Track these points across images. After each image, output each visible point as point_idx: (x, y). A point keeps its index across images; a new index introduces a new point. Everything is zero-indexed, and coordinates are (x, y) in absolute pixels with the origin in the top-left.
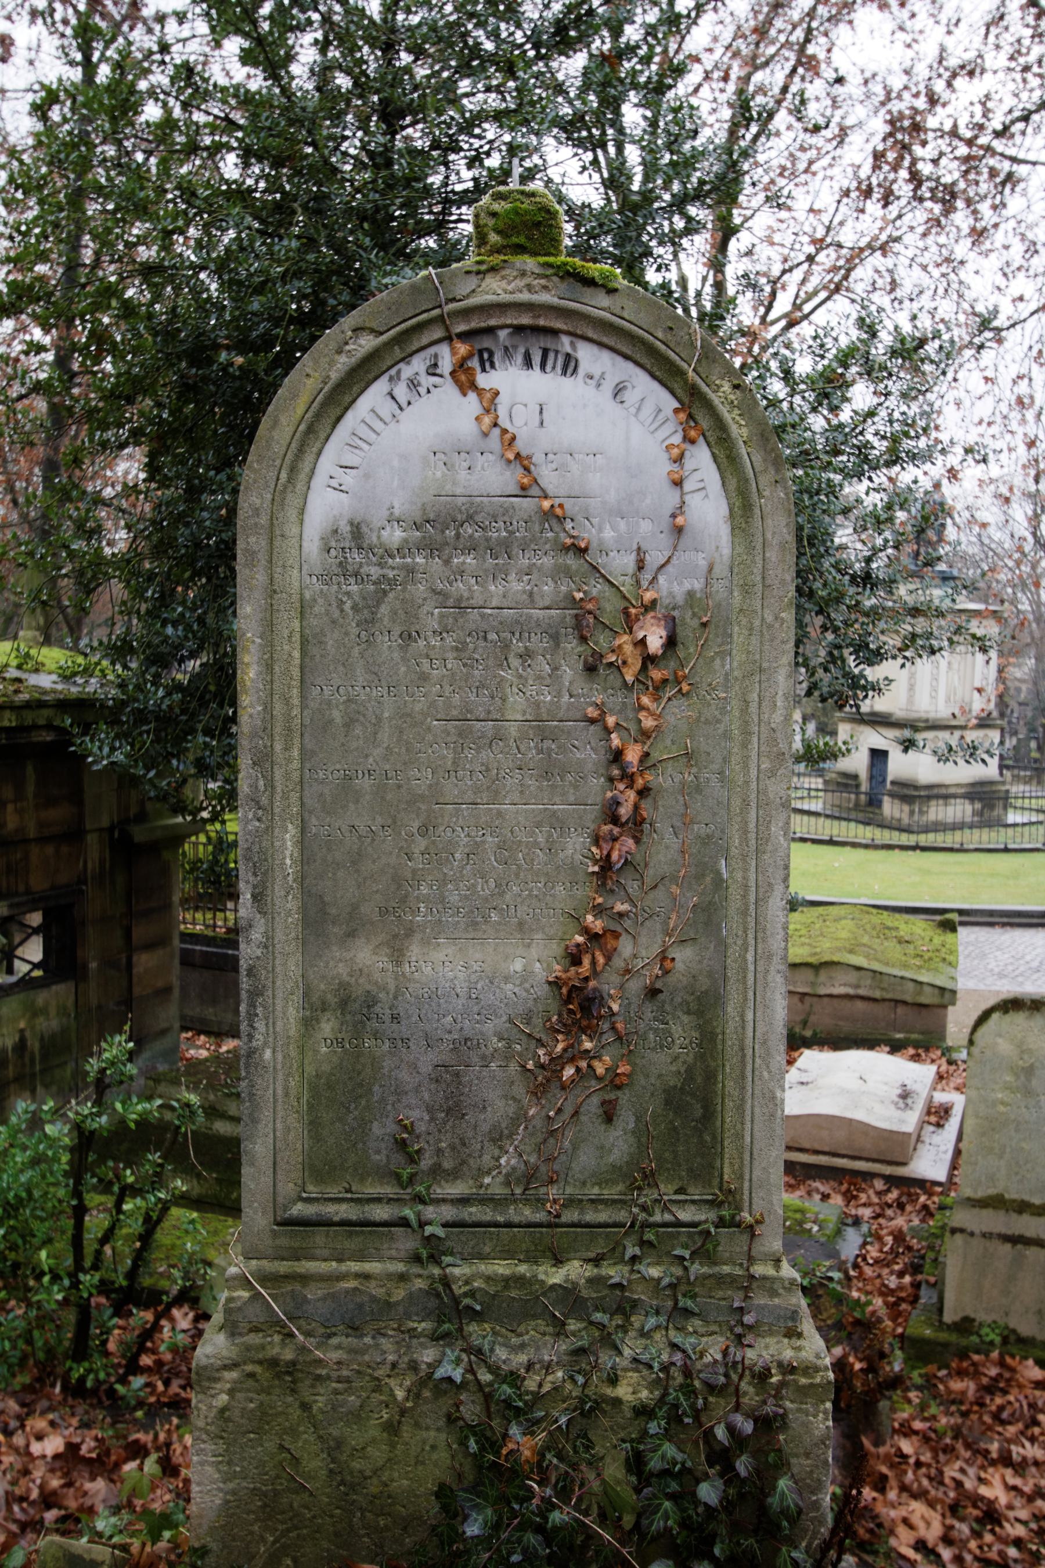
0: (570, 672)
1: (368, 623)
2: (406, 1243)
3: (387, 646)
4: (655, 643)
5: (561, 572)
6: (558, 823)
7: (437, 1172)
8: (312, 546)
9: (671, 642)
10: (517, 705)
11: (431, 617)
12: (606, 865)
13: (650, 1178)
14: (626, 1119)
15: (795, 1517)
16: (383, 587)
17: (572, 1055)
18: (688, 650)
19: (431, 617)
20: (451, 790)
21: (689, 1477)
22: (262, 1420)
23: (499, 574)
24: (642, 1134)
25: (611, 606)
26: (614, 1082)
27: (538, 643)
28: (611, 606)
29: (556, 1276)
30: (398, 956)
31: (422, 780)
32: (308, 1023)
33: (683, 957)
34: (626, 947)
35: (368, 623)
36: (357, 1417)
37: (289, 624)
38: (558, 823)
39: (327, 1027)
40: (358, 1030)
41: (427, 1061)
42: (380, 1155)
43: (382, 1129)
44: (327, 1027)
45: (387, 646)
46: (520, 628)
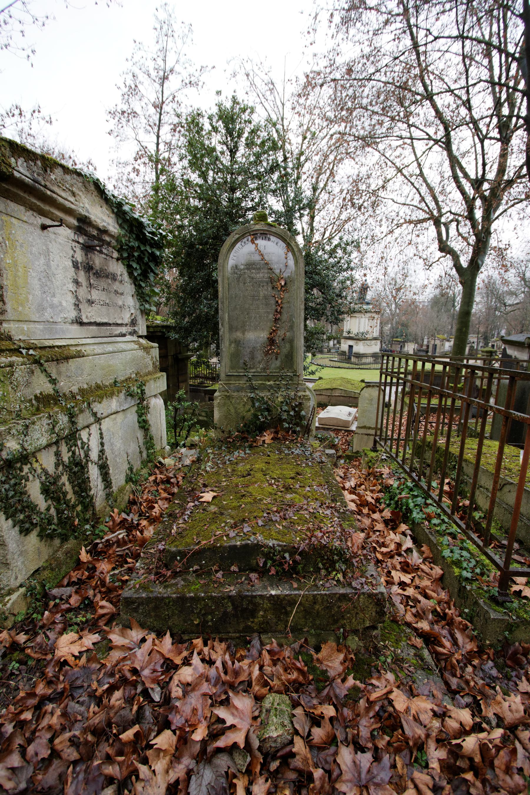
0: (270, 289)
1: (238, 281)
2: (246, 378)
3: (241, 284)
4: (283, 284)
5: (268, 273)
6: (268, 313)
7: (250, 368)
8: (229, 269)
9: (285, 284)
10: (262, 294)
11: (248, 280)
12: (276, 319)
13: (283, 369)
14: (279, 359)
15: (304, 416)
16: (241, 275)
17: (270, 349)
18: (288, 285)
19: (248, 280)
20: (252, 308)
21: (288, 412)
22: (224, 405)
23: (259, 273)
24: (282, 362)
25: (276, 278)
26: (277, 354)
27: (265, 284)
28: (276, 278)
29: (269, 383)
30: (244, 334)
31: (247, 306)
32: (230, 345)
33: (288, 334)
34: (279, 332)
35: (238, 281)
36: (239, 404)
37: (226, 281)
38: (268, 313)
39: (233, 345)
40: (238, 346)
41: (248, 350)
42: (242, 365)
43: (242, 361)
44: (233, 345)
45: (241, 284)
46: (262, 282)
